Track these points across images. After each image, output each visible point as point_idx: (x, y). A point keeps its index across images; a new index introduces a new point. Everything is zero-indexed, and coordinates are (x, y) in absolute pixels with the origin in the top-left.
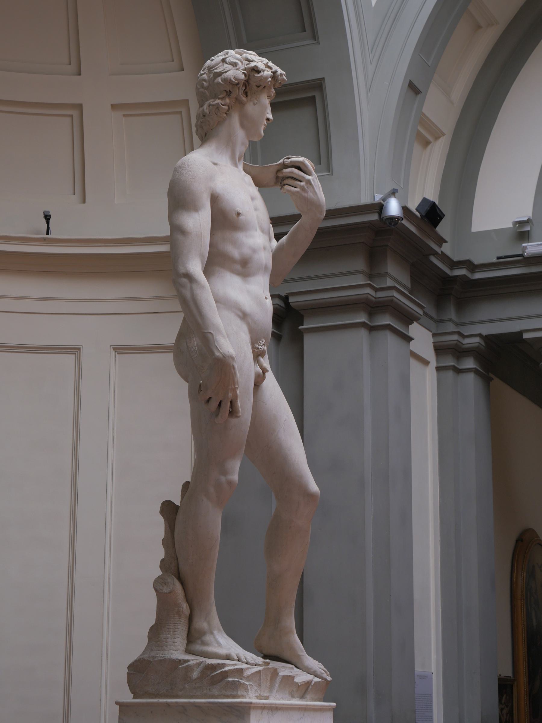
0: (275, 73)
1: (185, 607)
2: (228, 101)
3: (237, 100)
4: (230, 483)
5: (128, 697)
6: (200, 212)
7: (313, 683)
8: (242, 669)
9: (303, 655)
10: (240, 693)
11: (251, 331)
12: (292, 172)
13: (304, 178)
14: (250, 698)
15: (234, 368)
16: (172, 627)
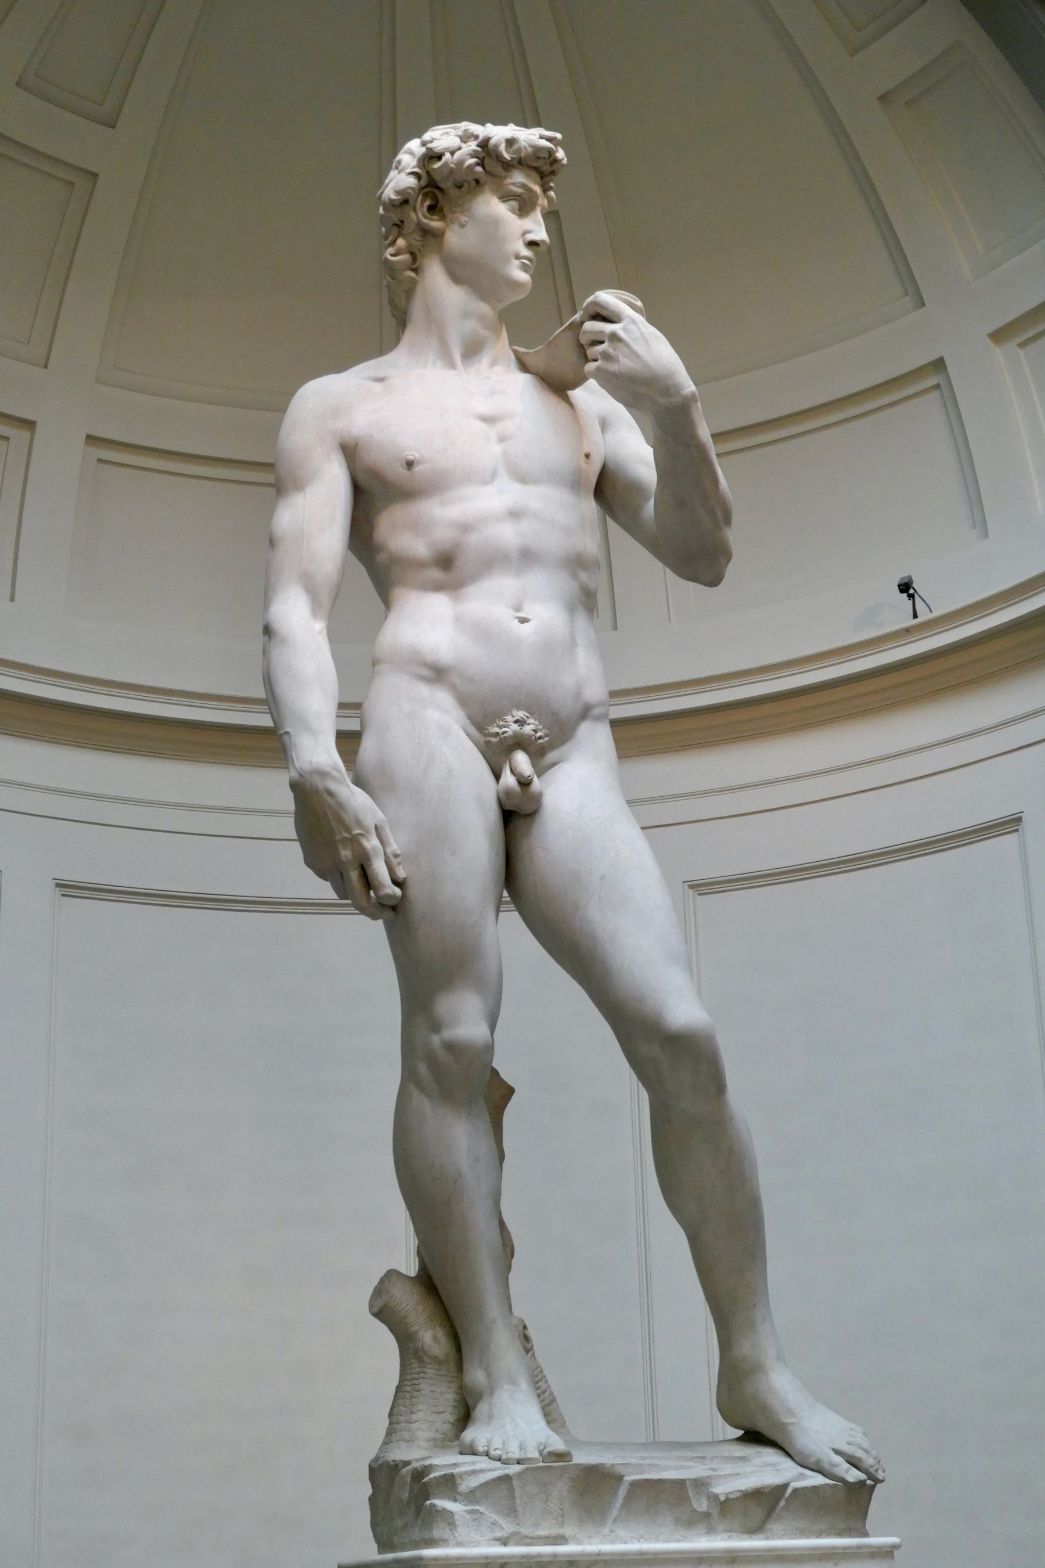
0: (485, 144)
1: (432, 1338)
2: (401, 242)
3: (426, 232)
4: (452, 1047)
5: (371, 1553)
6: (308, 490)
7: (789, 1490)
8: (452, 1475)
9: (793, 1423)
10: (436, 1534)
11: (463, 701)
12: (584, 332)
13: (602, 332)
14: (459, 1544)
15: (330, 794)
16: (408, 1389)
